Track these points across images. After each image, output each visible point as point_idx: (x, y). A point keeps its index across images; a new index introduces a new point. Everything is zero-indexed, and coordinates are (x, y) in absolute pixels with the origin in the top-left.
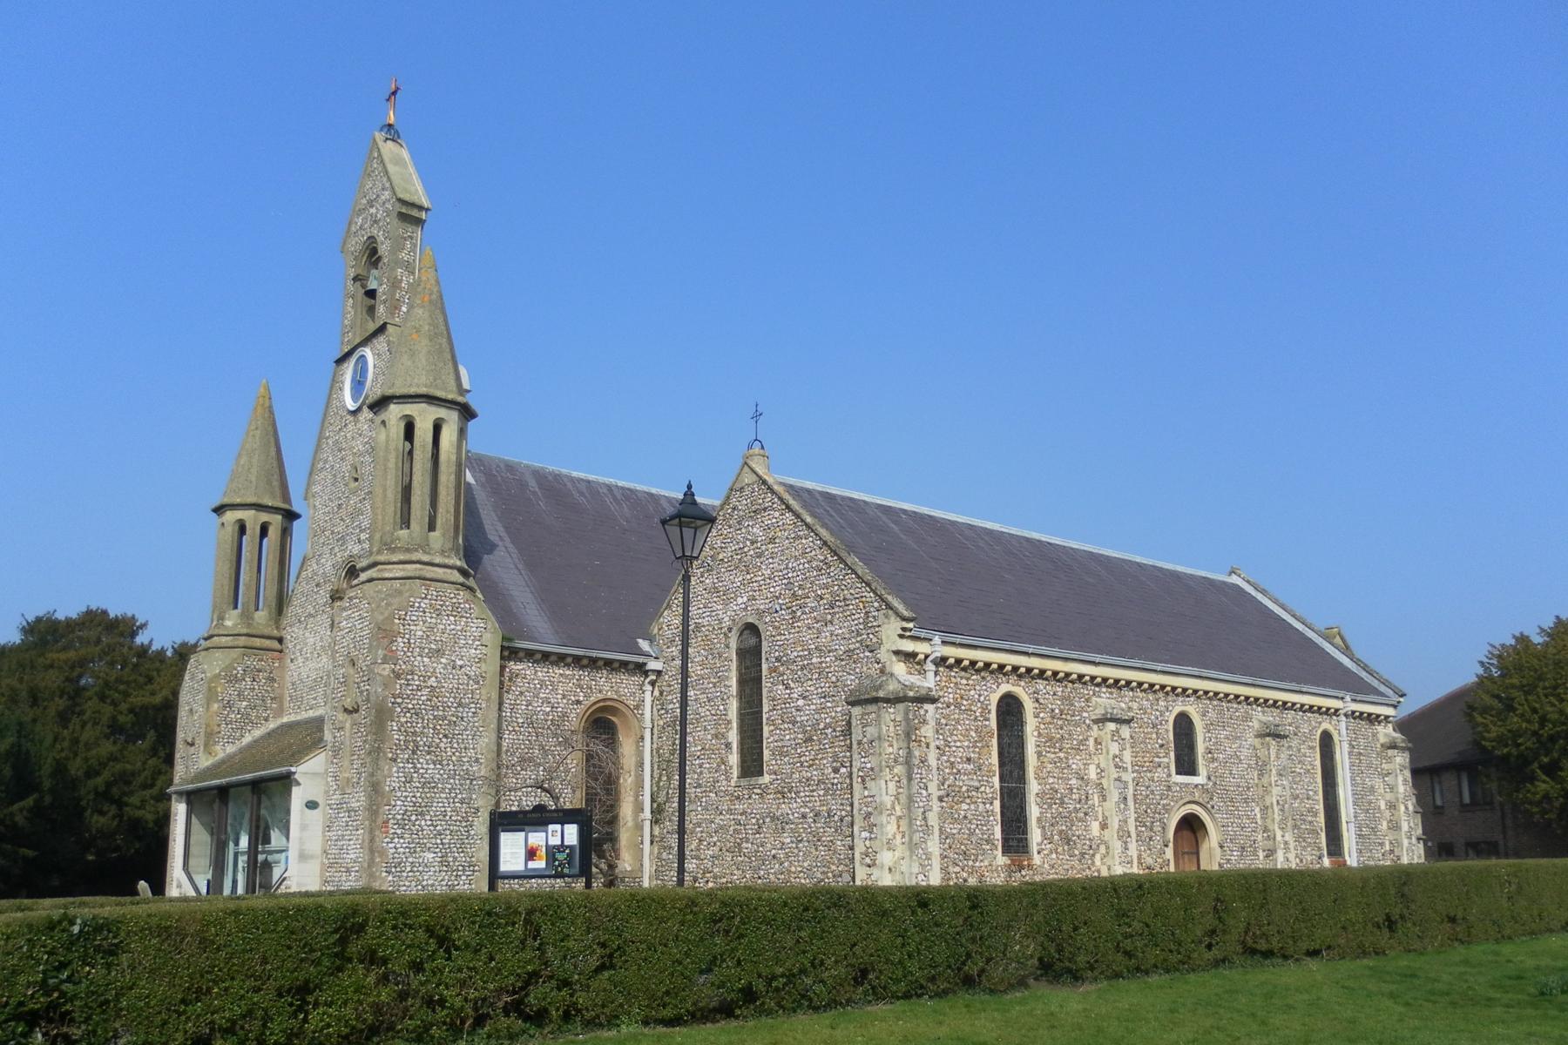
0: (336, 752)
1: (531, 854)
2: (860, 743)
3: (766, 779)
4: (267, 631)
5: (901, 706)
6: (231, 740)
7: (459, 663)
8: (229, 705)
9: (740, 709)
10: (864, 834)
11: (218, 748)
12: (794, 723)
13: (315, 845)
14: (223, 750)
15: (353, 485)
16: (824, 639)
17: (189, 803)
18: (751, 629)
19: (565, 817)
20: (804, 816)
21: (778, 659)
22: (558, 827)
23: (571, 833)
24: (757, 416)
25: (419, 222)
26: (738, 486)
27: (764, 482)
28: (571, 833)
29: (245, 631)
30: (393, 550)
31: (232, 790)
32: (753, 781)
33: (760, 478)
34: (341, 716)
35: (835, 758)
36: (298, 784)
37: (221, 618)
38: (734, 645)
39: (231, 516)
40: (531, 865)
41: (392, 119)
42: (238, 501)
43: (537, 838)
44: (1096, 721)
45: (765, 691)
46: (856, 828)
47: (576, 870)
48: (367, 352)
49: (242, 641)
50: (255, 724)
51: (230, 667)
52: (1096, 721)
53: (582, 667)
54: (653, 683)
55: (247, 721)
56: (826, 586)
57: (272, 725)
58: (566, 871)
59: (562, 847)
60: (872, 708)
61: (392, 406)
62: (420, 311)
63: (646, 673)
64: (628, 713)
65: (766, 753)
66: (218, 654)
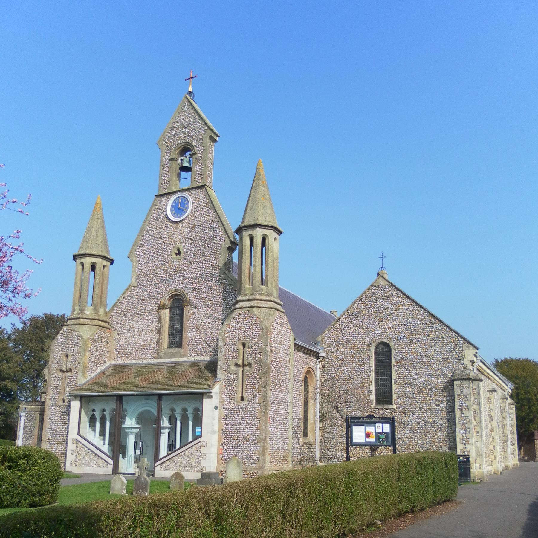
0: (228, 384)
1: (368, 435)
2: (459, 395)
3: (394, 406)
4: (104, 318)
5: (476, 382)
6: (93, 371)
7: (285, 348)
8: (92, 354)
9: (376, 376)
10: (462, 431)
11: (88, 374)
12: (412, 385)
13: (216, 427)
14: (90, 376)
15: (174, 256)
16: (431, 352)
17: (81, 402)
18: (386, 345)
19: (384, 420)
20: (418, 423)
21: (401, 358)
22: (380, 424)
23: (387, 428)
24: (383, 257)
25: (215, 141)
26: (376, 285)
27: (393, 285)
28: (387, 428)
29: (97, 317)
30: (261, 294)
31: (124, 398)
32: (386, 407)
33: (391, 283)
34: (233, 368)
35: (437, 400)
36: (211, 397)
37: (82, 310)
38: (373, 349)
39: (88, 261)
40: (368, 440)
41: (191, 89)
42: (95, 253)
43: (370, 429)
44: (488, 391)
45: (393, 371)
46: (457, 429)
47: (390, 443)
48: (186, 195)
49: (96, 322)
50: (101, 364)
51: (93, 335)
52: (488, 391)
53: (304, 353)
54: (319, 362)
55: (98, 363)
56: (432, 332)
57: (107, 365)
58: (385, 443)
59: (382, 433)
60: (465, 382)
61: (258, 229)
62: (263, 188)
63: (318, 358)
64: (313, 373)
65: (394, 396)
66: (85, 327)
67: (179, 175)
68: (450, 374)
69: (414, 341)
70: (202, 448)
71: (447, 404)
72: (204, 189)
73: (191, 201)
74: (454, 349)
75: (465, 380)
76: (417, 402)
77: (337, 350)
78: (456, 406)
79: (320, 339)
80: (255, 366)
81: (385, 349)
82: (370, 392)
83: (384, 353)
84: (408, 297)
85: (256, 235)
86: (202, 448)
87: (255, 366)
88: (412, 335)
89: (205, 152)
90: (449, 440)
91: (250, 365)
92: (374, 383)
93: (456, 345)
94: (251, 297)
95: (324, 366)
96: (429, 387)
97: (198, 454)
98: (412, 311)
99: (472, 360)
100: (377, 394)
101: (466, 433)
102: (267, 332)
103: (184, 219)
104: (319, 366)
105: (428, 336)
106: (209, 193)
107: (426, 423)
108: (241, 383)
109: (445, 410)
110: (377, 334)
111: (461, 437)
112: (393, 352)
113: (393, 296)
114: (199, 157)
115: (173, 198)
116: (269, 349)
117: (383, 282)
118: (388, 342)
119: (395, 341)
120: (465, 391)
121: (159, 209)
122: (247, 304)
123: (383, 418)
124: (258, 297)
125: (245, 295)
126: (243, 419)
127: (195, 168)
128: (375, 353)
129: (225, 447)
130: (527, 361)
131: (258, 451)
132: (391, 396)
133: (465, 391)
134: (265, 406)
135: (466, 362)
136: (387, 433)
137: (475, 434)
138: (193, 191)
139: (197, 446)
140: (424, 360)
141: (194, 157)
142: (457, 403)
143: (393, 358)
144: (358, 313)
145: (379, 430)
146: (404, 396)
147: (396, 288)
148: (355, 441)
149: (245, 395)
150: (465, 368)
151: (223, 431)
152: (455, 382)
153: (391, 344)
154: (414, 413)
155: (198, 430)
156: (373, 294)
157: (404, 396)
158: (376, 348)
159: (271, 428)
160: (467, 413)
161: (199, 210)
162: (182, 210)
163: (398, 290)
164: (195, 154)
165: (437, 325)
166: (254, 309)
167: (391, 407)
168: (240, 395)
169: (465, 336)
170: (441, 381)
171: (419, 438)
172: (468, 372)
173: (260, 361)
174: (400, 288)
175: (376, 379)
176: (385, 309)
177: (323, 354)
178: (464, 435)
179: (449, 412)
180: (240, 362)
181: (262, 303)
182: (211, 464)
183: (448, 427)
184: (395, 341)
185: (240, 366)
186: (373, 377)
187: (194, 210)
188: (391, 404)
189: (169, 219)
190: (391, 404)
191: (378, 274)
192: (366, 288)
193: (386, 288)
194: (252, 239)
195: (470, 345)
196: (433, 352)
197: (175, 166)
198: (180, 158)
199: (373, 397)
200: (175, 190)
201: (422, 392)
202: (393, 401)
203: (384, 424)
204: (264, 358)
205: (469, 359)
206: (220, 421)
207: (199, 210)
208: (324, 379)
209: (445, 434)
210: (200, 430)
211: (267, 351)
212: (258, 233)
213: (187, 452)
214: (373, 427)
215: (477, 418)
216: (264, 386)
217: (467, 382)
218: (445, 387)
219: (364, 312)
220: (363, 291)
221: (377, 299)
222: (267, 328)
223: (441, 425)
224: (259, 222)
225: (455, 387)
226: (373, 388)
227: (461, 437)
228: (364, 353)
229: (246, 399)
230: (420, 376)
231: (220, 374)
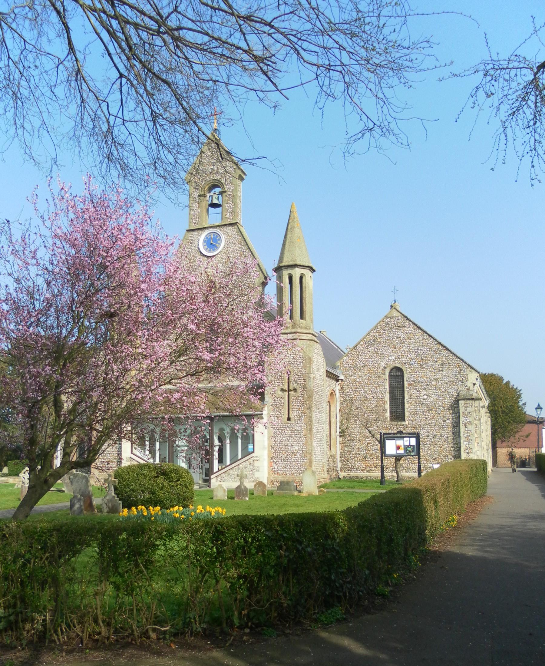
0: (275, 406)
1: (398, 448)
3: (407, 423)
9: (390, 397)
10: (465, 443)
12: (422, 404)
13: (266, 444)
18: (399, 369)
19: (411, 435)
21: (413, 381)
22: (408, 439)
23: (413, 441)
26: (390, 316)
27: (405, 317)
30: (301, 328)
32: (400, 423)
34: (280, 393)
35: (444, 417)
36: (262, 418)
43: (400, 443)
45: (406, 392)
46: (462, 441)
48: (217, 230)
56: (440, 358)
58: (412, 454)
59: (410, 446)
60: (468, 402)
61: (297, 269)
63: (337, 381)
65: (407, 414)
67: (208, 210)
68: (455, 395)
69: (424, 366)
70: (255, 462)
71: (453, 420)
72: (236, 227)
73: (223, 237)
74: (459, 373)
75: (469, 399)
76: (426, 418)
77: (355, 374)
78: (461, 422)
79: (339, 364)
80: (296, 389)
81: (398, 373)
82: (385, 410)
83: (397, 376)
84: (419, 328)
85: (295, 274)
86: (255, 462)
87: (300, 391)
88: (422, 362)
89: (235, 190)
90: (454, 450)
91: (295, 390)
92: (388, 402)
93: (461, 370)
94: (293, 330)
95: (342, 388)
96: (437, 406)
97: (251, 467)
98: (422, 340)
99: (474, 382)
100: (390, 412)
101: (469, 444)
102: (310, 362)
103: (217, 254)
104: (339, 388)
105: (436, 362)
106: (241, 230)
107: (434, 436)
108: (287, 406)
109: (450, 425)
110: (392, 359)
111: (465, 448)
112: (406, 376)
113: (405, 327)
114: (229, 195)
115: (205, 233)
116: (312, 376)
117: (396, 314)
118: (401, 367)
119: (407, 366)
120: (469, 409)
121: (191, 243)
122: (290, 336)
123: (410, 434)
124: (299, 330)
125: (287, 328)
126: (290, 436)
127: (226, 206)
128: (390, 376)
129: (275, 461)
130: (492, 375)
131: (306, 463)
132: (404, 413)
133: (469, 409)
134: (310, 425)
135: (469, 384)
136: (413, 446)
137: (476, 444)
138: (225, 228)
139: (251, 460)
140: (433, 383)
141: (224, 194)
142: (462, 419)
143: (405, 381)
144: (374, 341)
145: (407, 443)
146: (415, 414)
147: (408, 319)
148: (388, 452)
149: (291, 416)
150: (468, 389)
151: (272, 447)
152: (460, 402)
153: (404, 369)
154: (424, 428)
155: (250, 447)
156: (387, 324)
157: (415, 414)
158: (390, 372)
159: (315, 444)
160: (470, 427)
161: (232, 246)
162: (215, 246)
163: (410, 321)
164: (225, 192)
165: (444, 352)
166: (298, 341)
167: (403, 423)
168: (287, 416)
169: (468, 362)
170: (448, 401)
171: (428, 449)
172: (471, 393)
173: (305, 387)
174: (412, 320)
175: (390, 399)
176: (398, 338)
177: (342, 377)
178: (467, 446)
179: (454, 427)
180: (286, 388)
181: (303, 336)
182: (263, 474)
183: (453, 439)
184: (407, 366)
185: (286, 391)
186: (387, 397)
187: (227, 246)
188: (404, 421)
189: (201, 253)
190: (404, 421)
191: (392, 306)
192: (380, 319)
193: (398, 319)
194: (291, 278)
195: (472, 370)
196: (441, 376)
197: (205, 203)
198: (208, 195)
199: (388, 414)
200: (206, 226)
201: (431, 410)
202: (406, 418)
203: (411, 439)
204: (308, 384)
205: (471, 381)
206: (269, 438)
207: (232, 246)
208: (343, 399)
209: (451, 445)
210: (252, 447)
211: (311, 378)
212: (297, 273)
213: (241, 465)
214: (402, 441)
215: (478, 432)
216: (309, 408)
217: (471, 401)
218: (451, 406)
219: (379, 340)
220: (378, 322)
221: (391, 329)
222: (310, 358)
223: (448, 438)
224: (298, 263)
225: (460, 406)
226: (387, 406)
227: (465, 448)
228: (379, 377)
229: (292, 420)
230: (431, 396)
231: (268, 398)
